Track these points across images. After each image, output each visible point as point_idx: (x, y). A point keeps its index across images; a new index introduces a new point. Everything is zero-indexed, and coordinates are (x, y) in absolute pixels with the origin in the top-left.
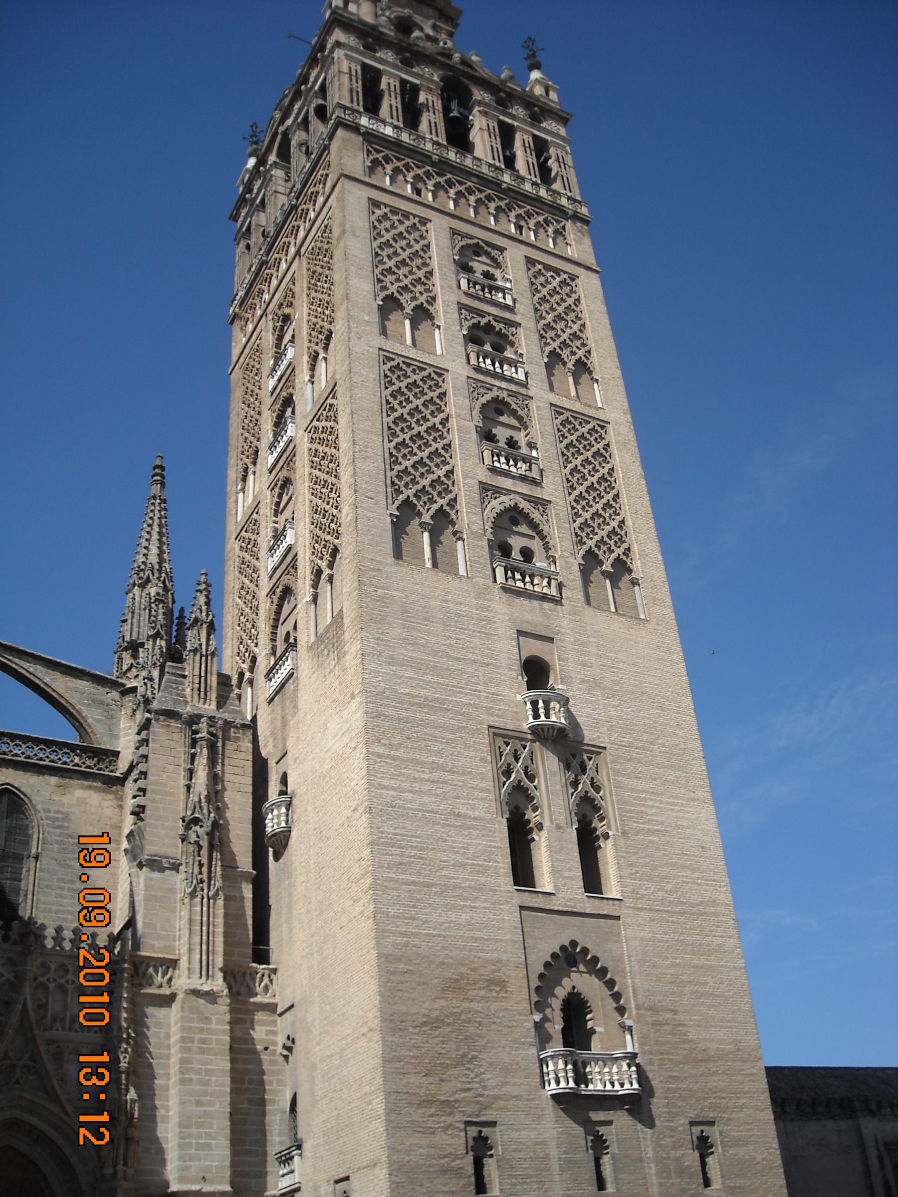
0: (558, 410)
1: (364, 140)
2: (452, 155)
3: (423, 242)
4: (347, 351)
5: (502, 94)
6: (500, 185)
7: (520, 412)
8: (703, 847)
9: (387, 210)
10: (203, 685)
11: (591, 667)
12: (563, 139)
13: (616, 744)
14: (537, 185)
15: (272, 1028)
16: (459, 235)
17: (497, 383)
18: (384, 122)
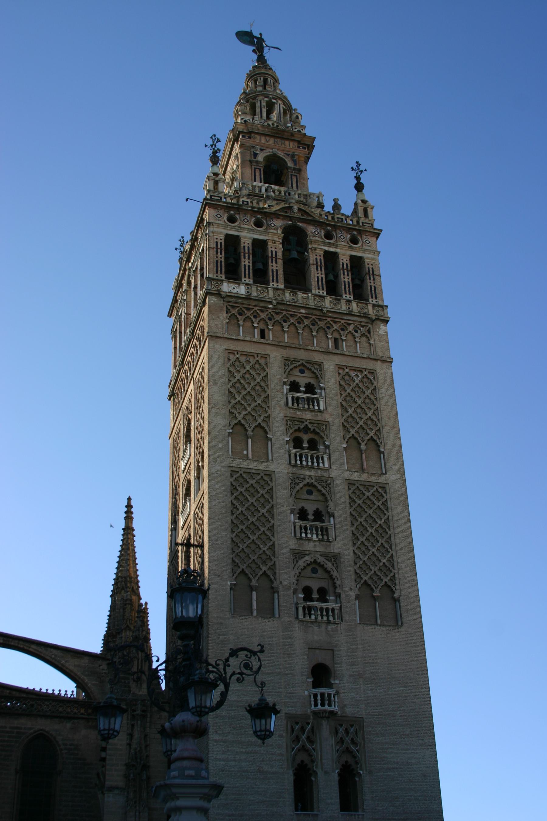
0: (351, 483)
1: (224, 301)
5: (329, 228)
6: (322, 310)
8: (425, 776)
9: (238, 356)
11: (357, 665)
13: (370, 715)
14: (349, 301)
16: (289, 360)
17: (307, 473)
18: (239, 284)
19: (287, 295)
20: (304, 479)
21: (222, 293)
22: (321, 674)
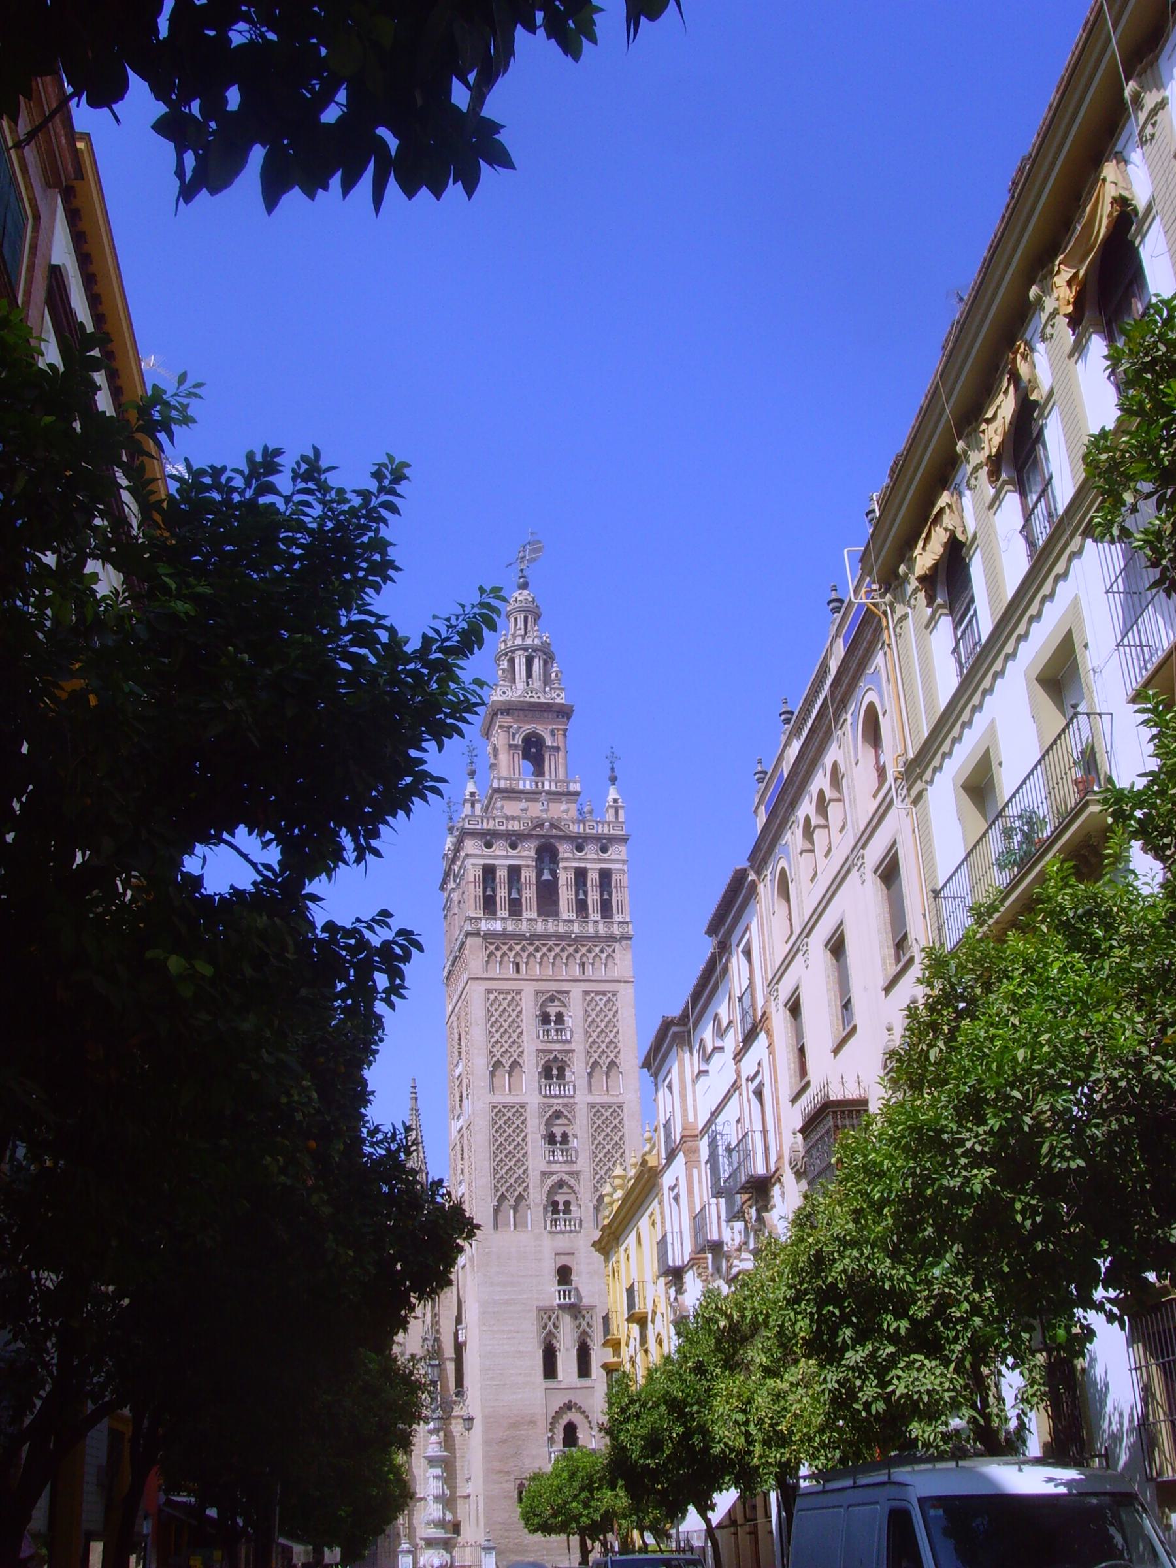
0: (592, 1106)
2: (539, 927)
3: (518, 1009)
12: (624, 862)
14: (597, 922)
19: (539, 923)
22: (564, 1275)
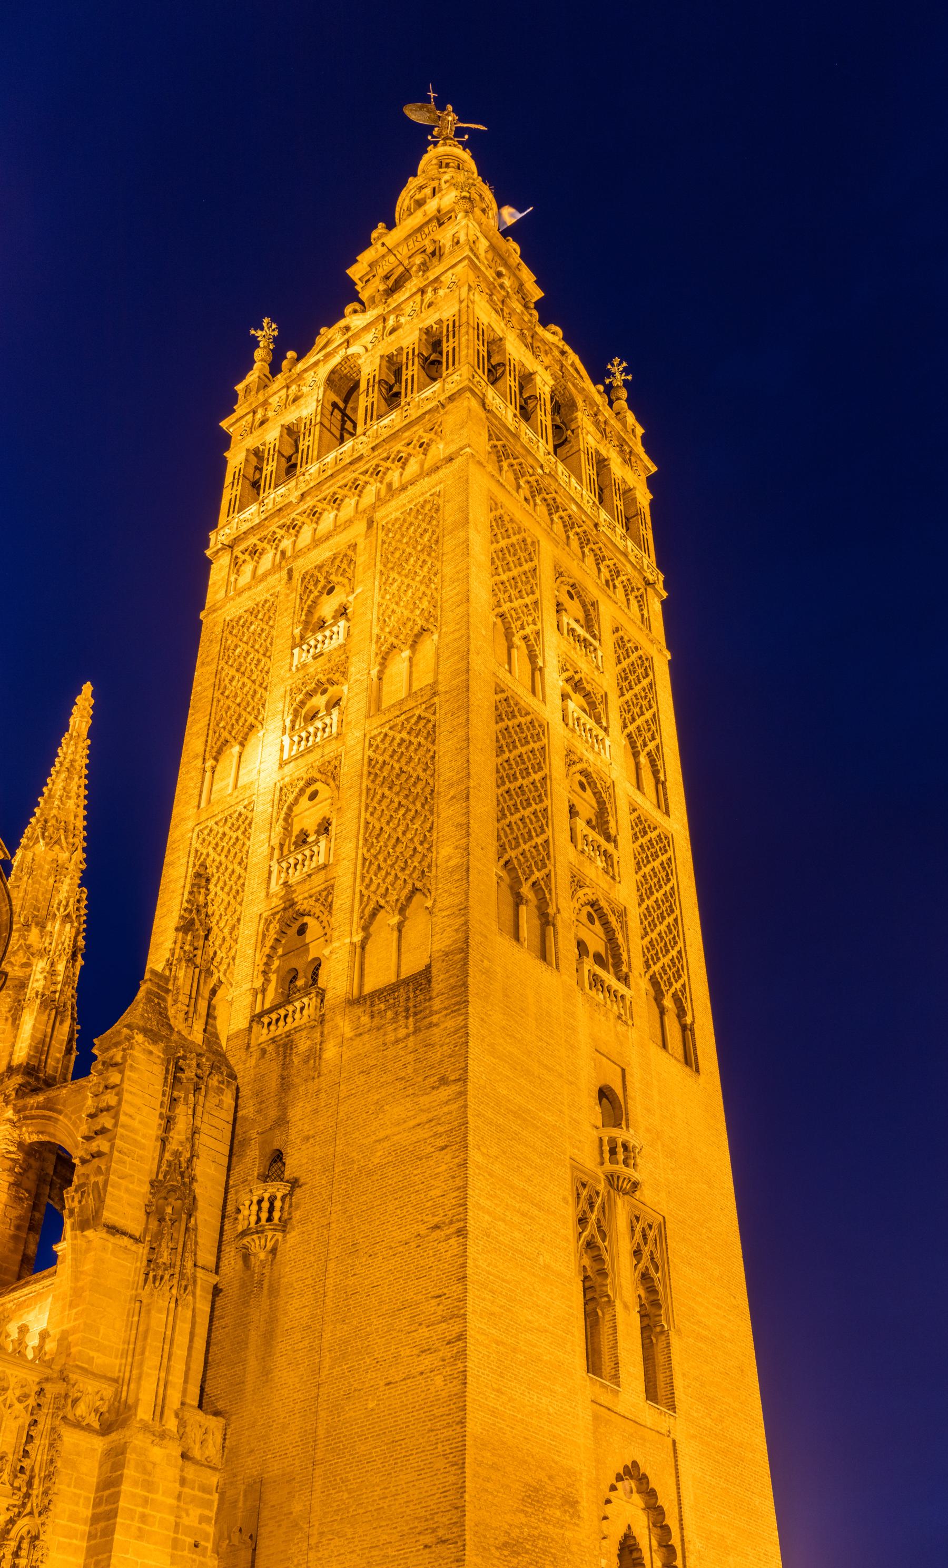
4: (465, 662)
6: (596, 525)
7: (603, 795)
10: (192, 1009)
15: (207, 1512)
20: (581, 760)
21: (487, 401)
